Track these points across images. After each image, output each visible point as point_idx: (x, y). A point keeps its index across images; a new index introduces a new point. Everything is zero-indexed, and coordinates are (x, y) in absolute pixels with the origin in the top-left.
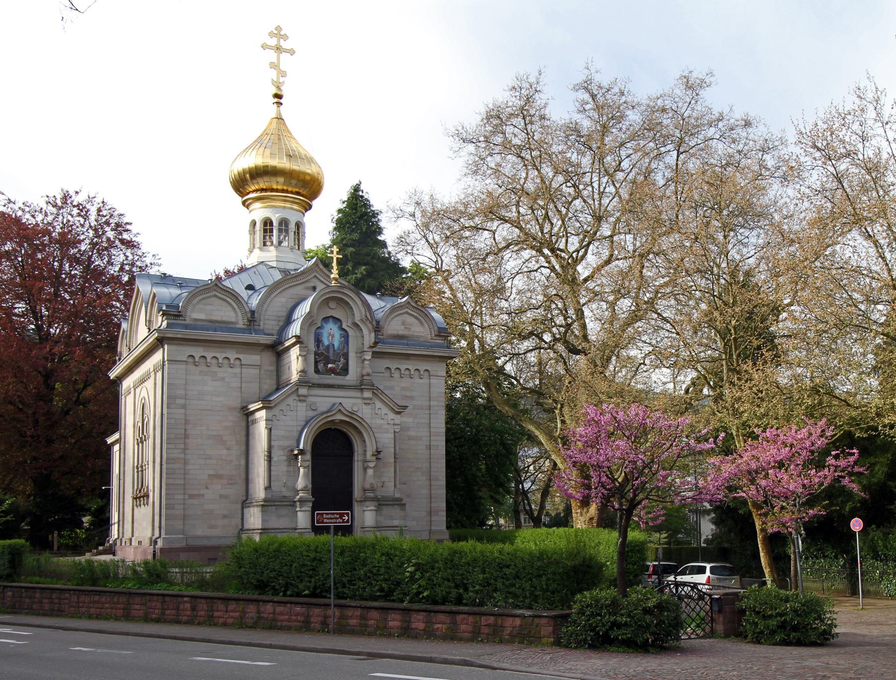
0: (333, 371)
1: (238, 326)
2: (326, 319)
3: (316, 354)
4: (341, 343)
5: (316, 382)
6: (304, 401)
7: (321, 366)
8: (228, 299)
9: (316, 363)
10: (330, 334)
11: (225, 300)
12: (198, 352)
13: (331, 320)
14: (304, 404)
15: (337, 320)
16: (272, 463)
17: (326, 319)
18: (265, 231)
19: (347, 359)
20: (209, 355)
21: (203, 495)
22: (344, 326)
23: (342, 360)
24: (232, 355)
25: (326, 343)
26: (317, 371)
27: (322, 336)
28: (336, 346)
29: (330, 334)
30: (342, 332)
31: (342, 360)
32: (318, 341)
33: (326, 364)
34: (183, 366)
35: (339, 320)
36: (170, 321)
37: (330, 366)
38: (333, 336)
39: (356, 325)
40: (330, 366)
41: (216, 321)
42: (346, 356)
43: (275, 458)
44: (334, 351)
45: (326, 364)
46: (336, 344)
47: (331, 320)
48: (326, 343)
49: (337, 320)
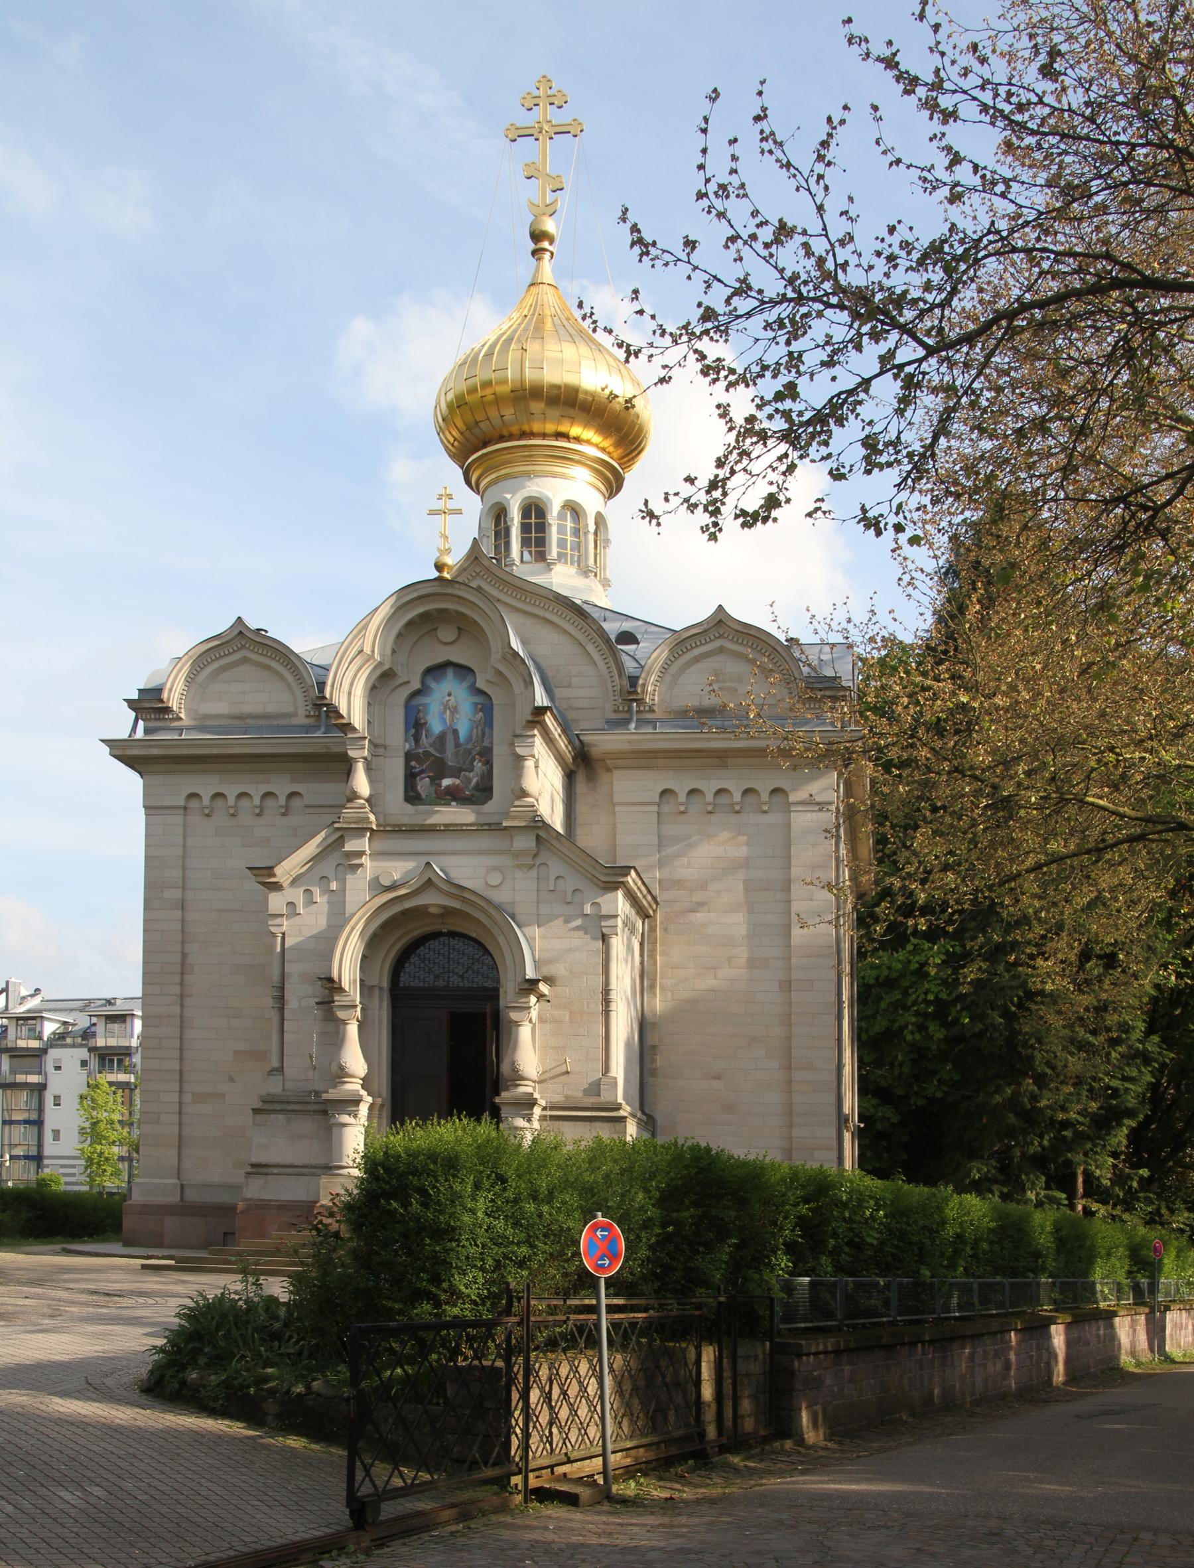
0: (454, 796)
1: (295, 721)
2: (435, 671)
3: (409, 756)
4: (474, 724)
5: (406, 820)
8: (274, 664)
9: (410, 778)
10: (446, 706)
11: (268, 668)
12: (206, 785)
13: (450, 672)
15: (464, 671)
16: (286, 1015)
17: (435, 671)
19: (489, 763)
20: (232, 791)
21: (223, 1095)
23: (478, 765)
24: (282, 786)
25: (436, 727)
26: (412, 797)
27: (426, 714)
28: (462, 736)
29: (446, 706)
30: (477, 699)
31: (478, 765)
32: (415, 724)
33: (436, 779)
34: (178, 819)
35: (469, 670)
36: (151, 724)
37: (446, 782)
38: (455, 711)
40: (446, 782)
41: (250, 716)
42: (486, 755)
43: (292, 1004)
44: (457, 745)
45: (436, 779)
46: (463, 729)
47: (450, 672)
48: (436, 727)
49: (464, 671)
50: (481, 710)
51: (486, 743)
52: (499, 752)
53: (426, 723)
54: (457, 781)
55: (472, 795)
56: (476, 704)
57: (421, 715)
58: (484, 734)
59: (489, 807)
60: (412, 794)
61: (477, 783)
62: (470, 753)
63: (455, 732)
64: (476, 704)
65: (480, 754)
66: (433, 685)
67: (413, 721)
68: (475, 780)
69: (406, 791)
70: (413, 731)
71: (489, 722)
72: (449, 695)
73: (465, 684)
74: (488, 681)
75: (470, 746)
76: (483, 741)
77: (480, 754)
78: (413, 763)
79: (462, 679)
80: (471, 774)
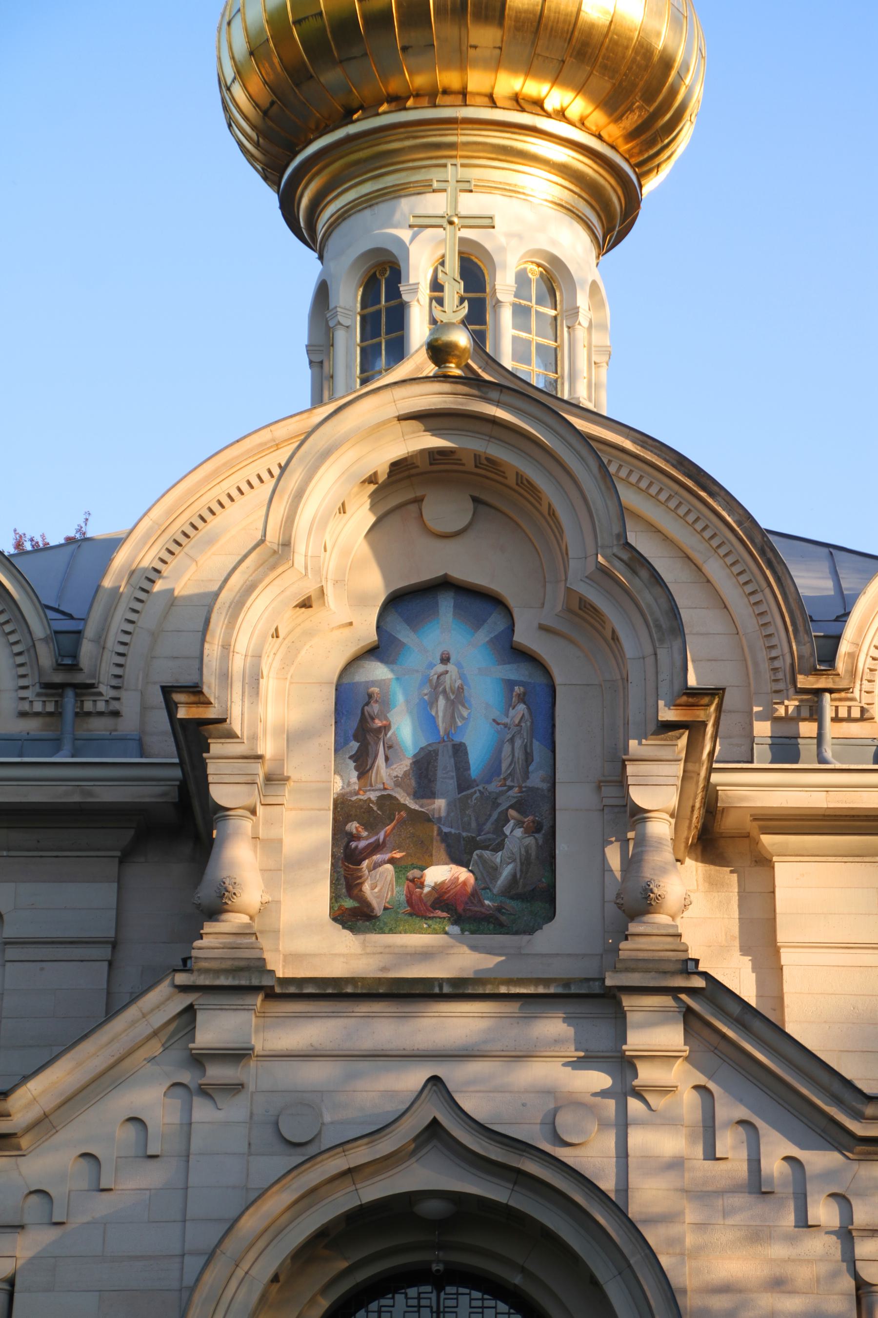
6: (237, 1088)
7: (380, 884)
9: (348, 862)
13: (446, 604)
14: (234, 1110)
18: (370, 325)
19: (546, 833)
22: (523, 636)
23: (516, 836)
29: (437, 687)
33: (408, 871)
38: (457, 698)
39: (582, 611)
44: (464, 783)
45: (408, 871)
46: (478, 742)
47: (446, 604)
50: (522, 699)
51: (537, 779)
52: (573, 800)
53: (386, 728)
54: (463, 874)
55: (499, 909)
56: (510, 684)
57: (375, 708)
58: (528, 758)
59: (549, 939)
60: (349, 903)
61: (514, 880)
62: (495, 805)
63: (459, 751)
64: (510, 684)
65: (520, 806)
66: (404, 634)
67: (353, 724)
68: (506, 872)
69: (335, 897)
70: (354, 745)
71: (545, 728)
72: (445, 660)
73: (483, 636)
74: (543, 628)
75: (494, 787)
76: (526, 775)
77: (520, 806)
78: (353, 826)
79: (477, 623)
80: (498, 857)
